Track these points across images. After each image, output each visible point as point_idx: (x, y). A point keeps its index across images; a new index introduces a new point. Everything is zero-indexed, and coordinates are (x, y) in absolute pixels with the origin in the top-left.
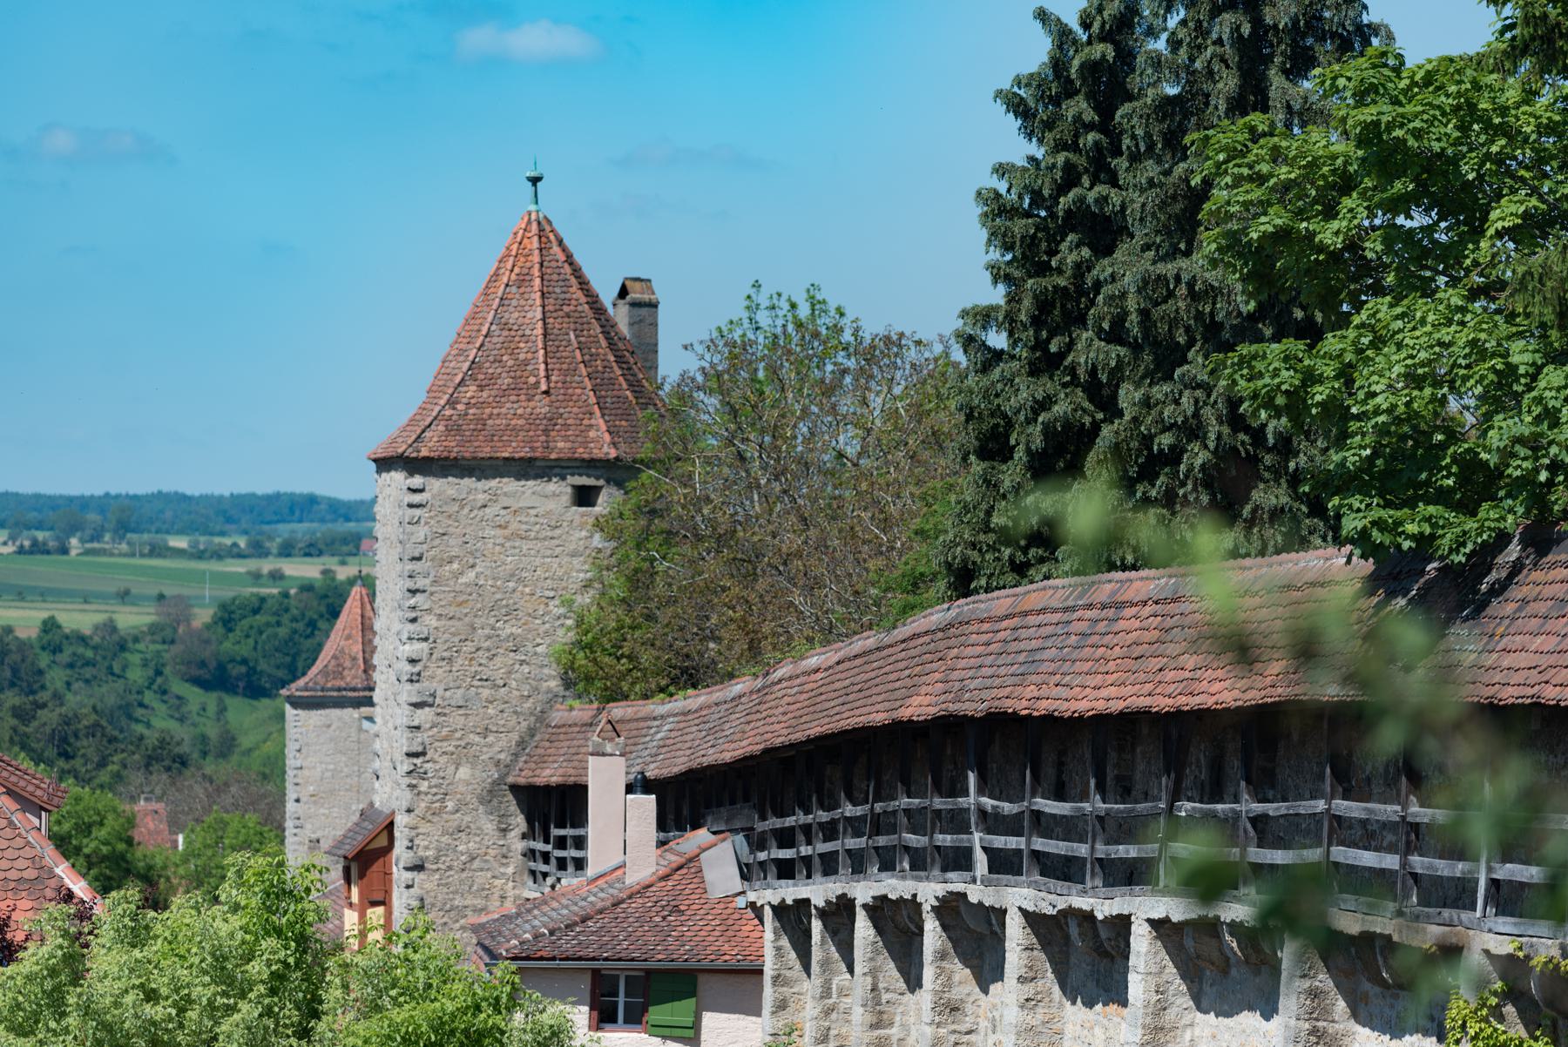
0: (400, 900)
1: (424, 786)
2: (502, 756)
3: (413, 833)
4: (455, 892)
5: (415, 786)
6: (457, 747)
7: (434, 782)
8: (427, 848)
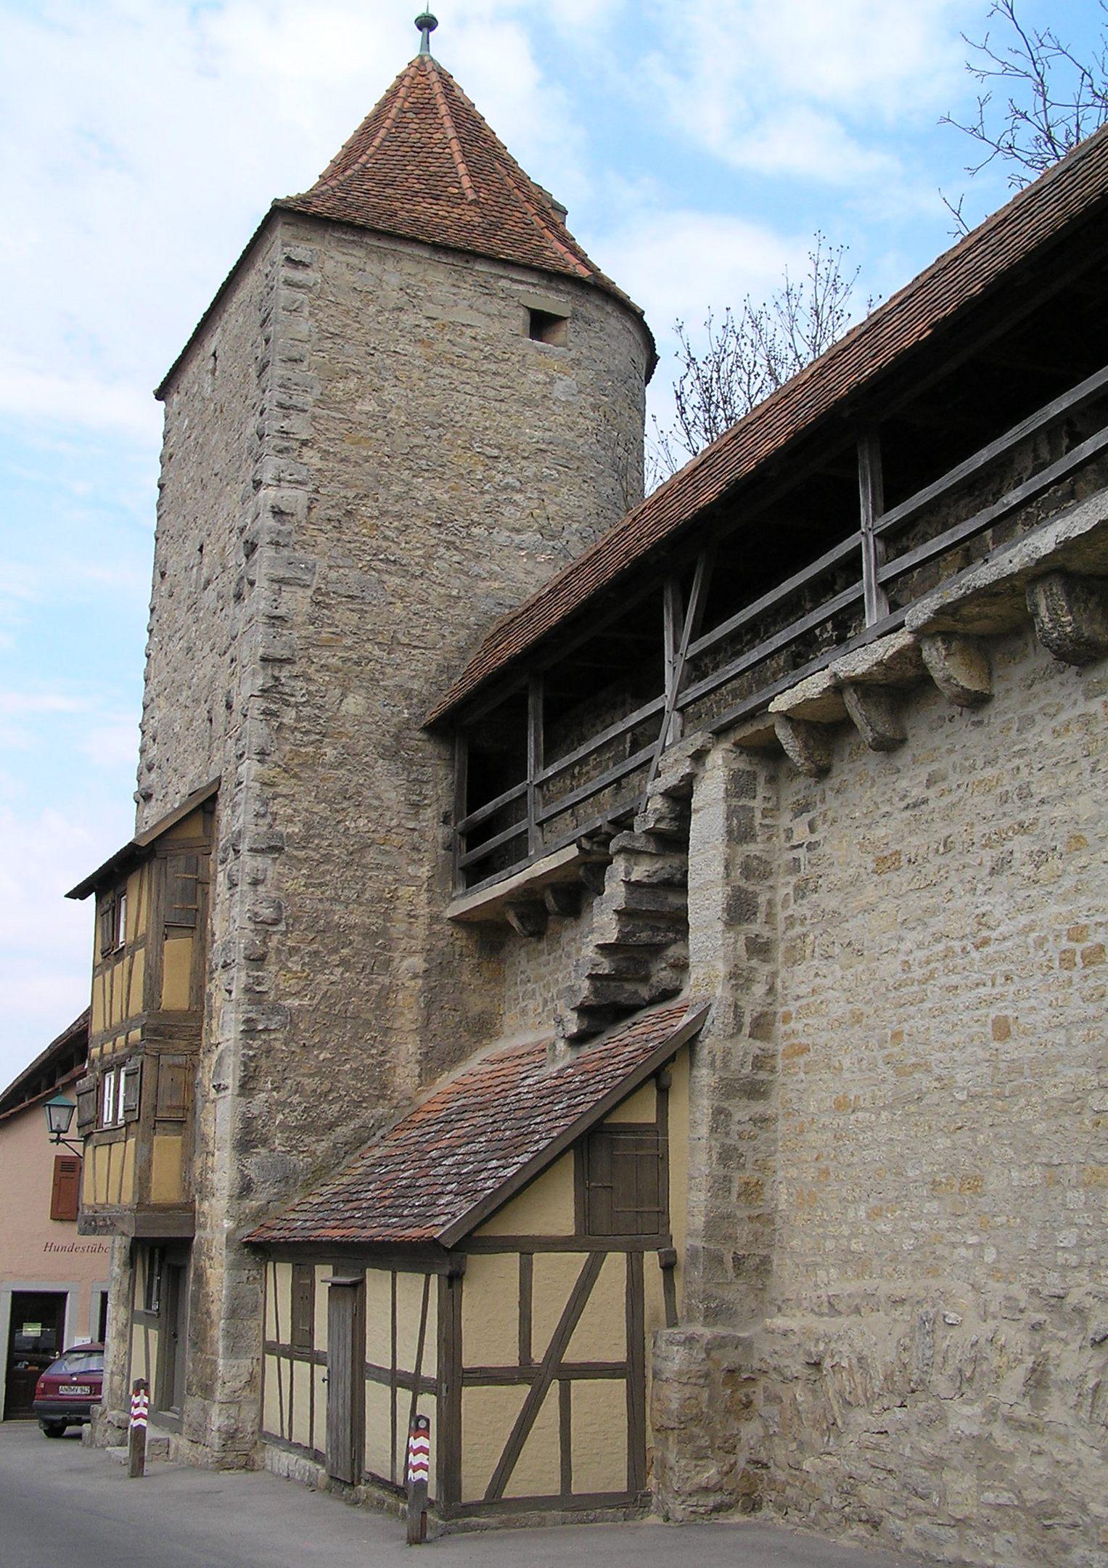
0: (230, 918)
1: (289, 717)
2: (416, 685)
3: (269, 792)
4: (335, 900)
5: (274, 714)
6: (345, 660)
7: (307, 711)
8: (290, 820)
